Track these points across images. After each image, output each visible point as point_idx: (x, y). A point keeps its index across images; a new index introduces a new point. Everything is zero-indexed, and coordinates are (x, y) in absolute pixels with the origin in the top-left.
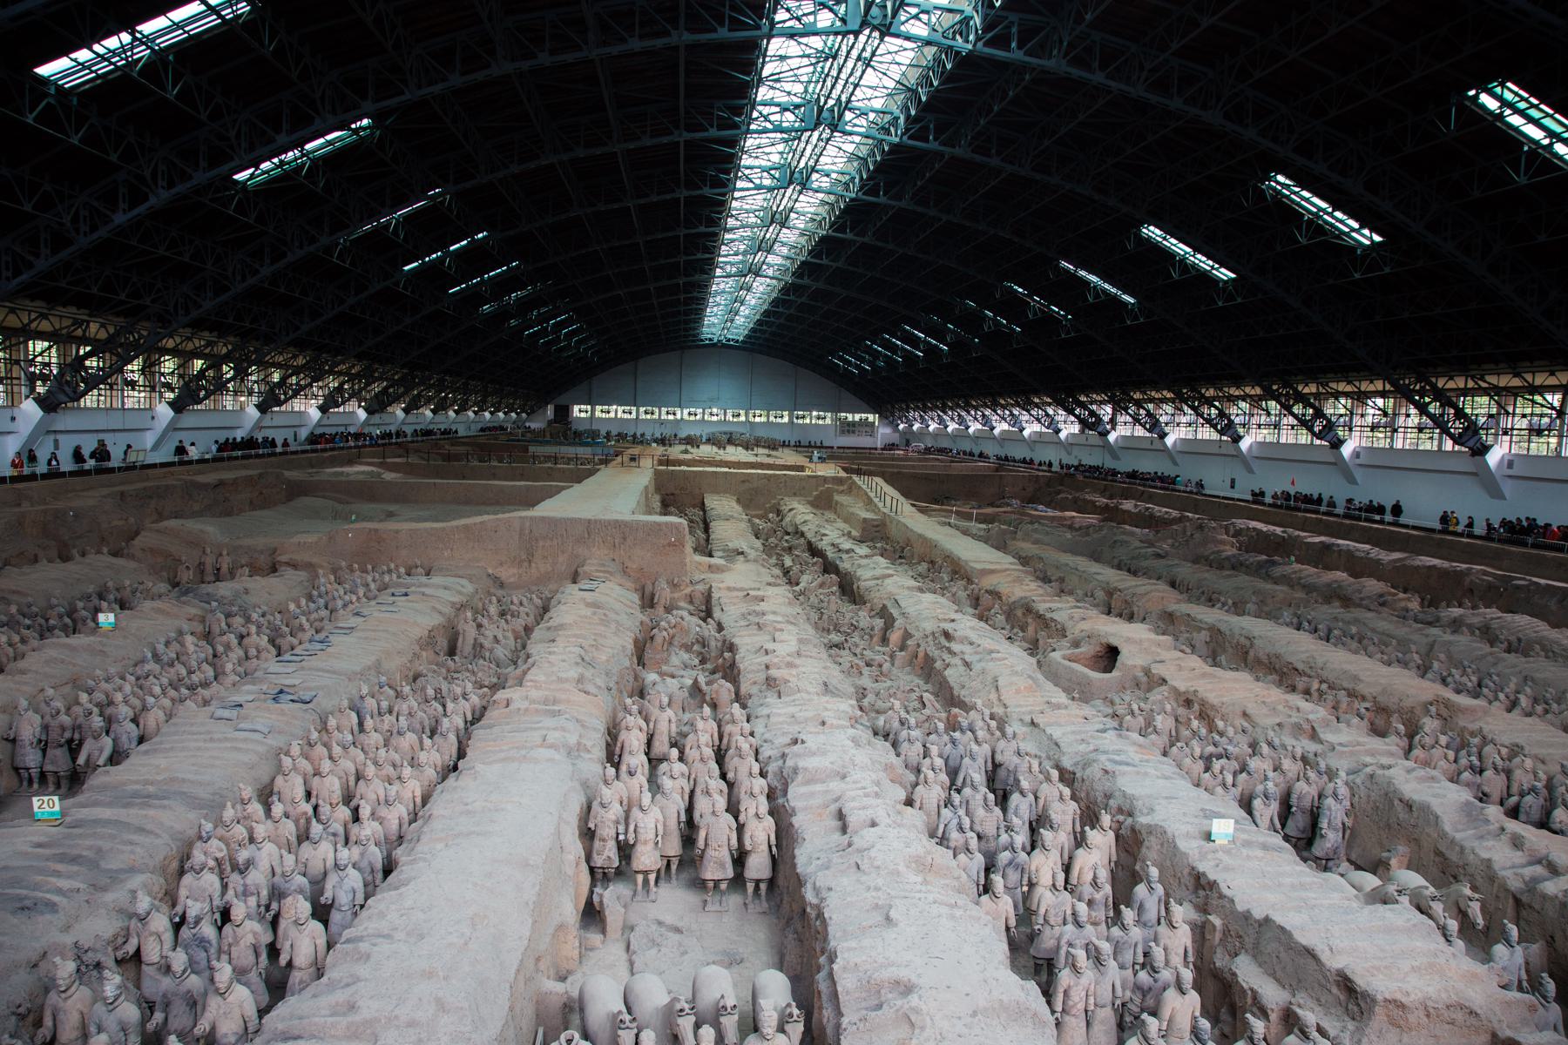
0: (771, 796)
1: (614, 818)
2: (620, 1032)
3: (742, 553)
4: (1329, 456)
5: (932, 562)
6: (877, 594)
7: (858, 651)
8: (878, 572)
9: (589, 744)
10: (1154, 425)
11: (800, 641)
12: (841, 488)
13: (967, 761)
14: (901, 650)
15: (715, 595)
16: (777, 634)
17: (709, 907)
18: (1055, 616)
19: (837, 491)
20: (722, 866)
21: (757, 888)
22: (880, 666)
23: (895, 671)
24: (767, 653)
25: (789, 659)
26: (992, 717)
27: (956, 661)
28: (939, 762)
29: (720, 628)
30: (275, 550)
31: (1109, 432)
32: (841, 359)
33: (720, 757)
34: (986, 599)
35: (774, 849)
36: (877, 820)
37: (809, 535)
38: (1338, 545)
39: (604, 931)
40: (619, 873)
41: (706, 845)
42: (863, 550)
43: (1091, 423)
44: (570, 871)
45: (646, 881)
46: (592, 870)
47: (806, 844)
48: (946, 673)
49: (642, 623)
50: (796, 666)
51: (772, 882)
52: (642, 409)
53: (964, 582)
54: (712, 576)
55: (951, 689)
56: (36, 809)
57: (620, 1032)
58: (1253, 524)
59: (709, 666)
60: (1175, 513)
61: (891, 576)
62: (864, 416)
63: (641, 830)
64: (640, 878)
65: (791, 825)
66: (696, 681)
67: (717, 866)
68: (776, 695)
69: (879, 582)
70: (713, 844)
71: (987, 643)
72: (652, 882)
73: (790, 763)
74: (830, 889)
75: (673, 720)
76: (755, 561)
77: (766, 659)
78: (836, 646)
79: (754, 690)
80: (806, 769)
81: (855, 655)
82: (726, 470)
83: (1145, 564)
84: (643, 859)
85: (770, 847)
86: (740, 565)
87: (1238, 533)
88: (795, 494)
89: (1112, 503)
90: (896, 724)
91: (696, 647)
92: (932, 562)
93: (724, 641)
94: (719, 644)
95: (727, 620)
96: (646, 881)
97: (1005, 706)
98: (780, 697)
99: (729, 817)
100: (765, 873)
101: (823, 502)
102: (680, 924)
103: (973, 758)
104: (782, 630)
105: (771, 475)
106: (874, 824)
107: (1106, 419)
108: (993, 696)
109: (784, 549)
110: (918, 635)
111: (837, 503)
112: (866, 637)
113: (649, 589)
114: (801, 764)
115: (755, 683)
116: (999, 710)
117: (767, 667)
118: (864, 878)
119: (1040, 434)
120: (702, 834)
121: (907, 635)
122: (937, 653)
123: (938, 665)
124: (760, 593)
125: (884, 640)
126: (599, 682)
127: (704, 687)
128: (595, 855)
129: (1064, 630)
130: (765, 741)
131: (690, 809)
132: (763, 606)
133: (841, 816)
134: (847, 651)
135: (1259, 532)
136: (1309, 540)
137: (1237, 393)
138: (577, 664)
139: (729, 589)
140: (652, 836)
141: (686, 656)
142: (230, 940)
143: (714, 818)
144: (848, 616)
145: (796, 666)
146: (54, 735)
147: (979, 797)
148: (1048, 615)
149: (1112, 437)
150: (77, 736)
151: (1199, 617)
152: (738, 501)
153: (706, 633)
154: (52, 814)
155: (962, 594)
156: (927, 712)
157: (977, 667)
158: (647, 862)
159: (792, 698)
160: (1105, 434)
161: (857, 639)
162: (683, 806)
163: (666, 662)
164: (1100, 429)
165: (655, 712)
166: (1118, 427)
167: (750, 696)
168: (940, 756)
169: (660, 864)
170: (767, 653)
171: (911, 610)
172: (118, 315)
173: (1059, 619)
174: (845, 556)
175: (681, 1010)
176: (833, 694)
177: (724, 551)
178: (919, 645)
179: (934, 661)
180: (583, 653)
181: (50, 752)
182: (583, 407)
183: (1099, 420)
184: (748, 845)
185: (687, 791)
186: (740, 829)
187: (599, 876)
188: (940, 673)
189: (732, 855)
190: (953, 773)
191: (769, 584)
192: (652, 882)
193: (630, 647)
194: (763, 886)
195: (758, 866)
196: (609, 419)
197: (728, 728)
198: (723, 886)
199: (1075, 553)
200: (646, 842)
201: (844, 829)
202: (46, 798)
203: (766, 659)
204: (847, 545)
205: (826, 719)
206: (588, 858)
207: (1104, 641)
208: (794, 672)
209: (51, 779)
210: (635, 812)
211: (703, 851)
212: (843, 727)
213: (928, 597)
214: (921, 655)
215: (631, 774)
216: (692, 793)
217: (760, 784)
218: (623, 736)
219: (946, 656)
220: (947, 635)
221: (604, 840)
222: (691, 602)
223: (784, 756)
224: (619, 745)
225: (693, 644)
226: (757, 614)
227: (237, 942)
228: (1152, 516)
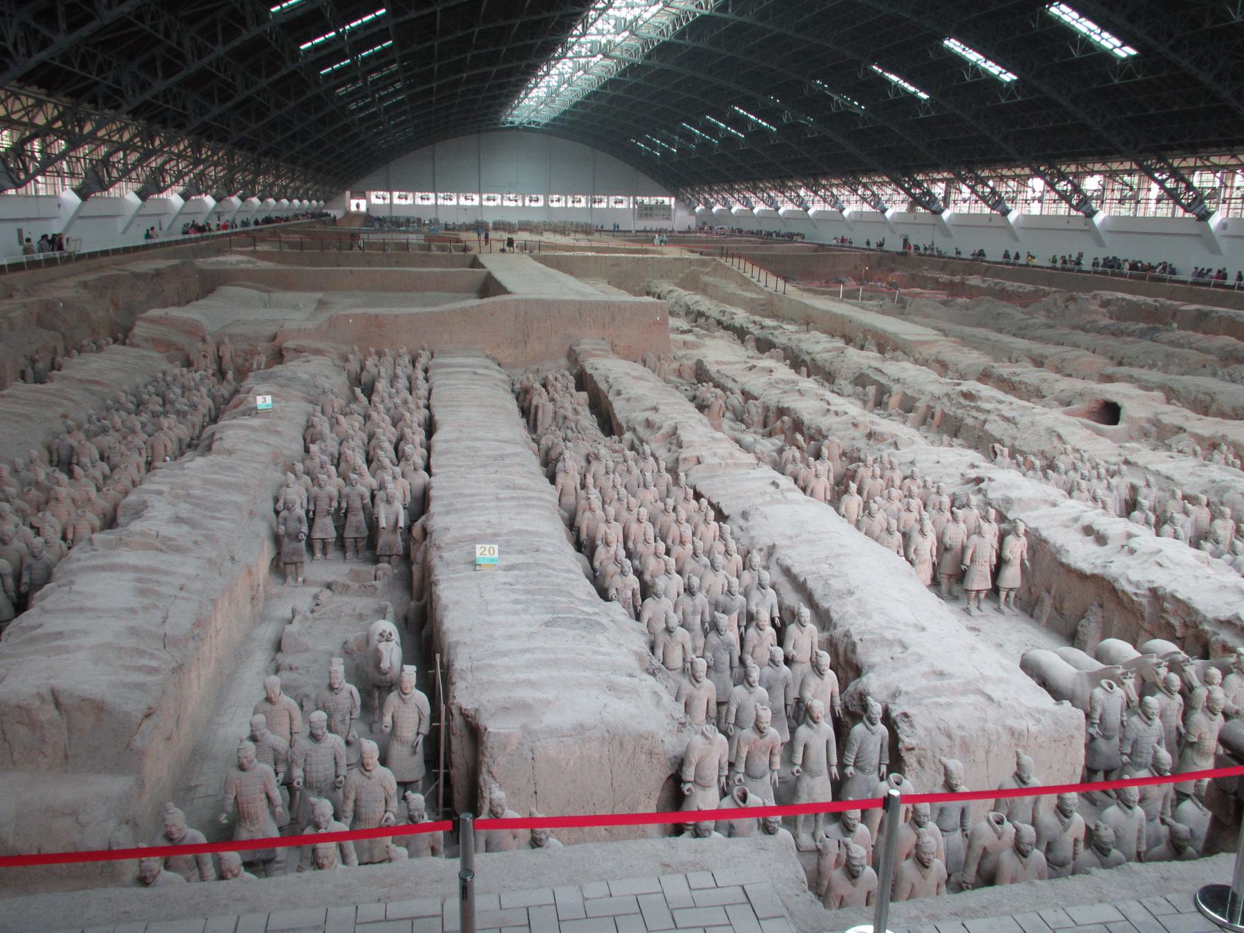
1: (897, 543)
4: (1196, 228)
10: (996, 201)
12: (709, 269)
15: (712, 369)
18: (1025, 380)
19: (702, 272)
20: (987, 580)
21: (1007, 596)
24: (837, 413)
27: (992, 417)
29: (747, 395)
30: (274, 338)
31: (942, 211)
32: (649, 143)
35: (1027, 562)
38: (1217, 312)
41: (972, 560)
43: (923, 200)
52: (485, 196)
53: (899, 353)
56: (478, 555)
57: (1125, 681)
58: (1120, 295)
60: (1029, 288)
62: (660, 199)
65: (1045, 541)
67: (980, 580)
70: (979, 560)
80: (1020, 499)
82: (594, 254)
83: (1038, 333)
85: (1022, 560)
87: (1106, 304)
88: (662, 277)
89: (957, 279)
93: (767, 409)
94: (760, 410)
98: (897, 449)
101: (691, 283)
105: (639, 259)
107: (940, 197)
111: (706, 285)
117: (855, 425)
119: (861, 214)
133: (1088, 530)
135: (1129, 302)
136: (1184, 308)
137: (1121, 167)
142: (755, 642)
146: (323, 505)
148: (1014, 379)
149: (946, 215)
150: (344, 505)
151: (1144, 377)
152: (609, 283)
154: (492, 560)
157: (1024, 420)
160: (938, 212)
164: (934, 208)
166: (952, 205)
172: (66, 96)
173: (1029, 382)
174: (775, 332)
181: (319, 522)
182: (381, 193)
183: (933, 199)
189: (991, 571)
194: (1012, 594)
195: (1012, 577)
196: (473, 207)
198: (982, 595)
199: (979, 325)
200: (924, 562)
202: (488, 546)
204: (768, 322)
205: (976, 463)
207: (1100, 398)
209: (318, 546)
214: (938, 415)
219: (975, 414)
220: (967, 396)
222: (680, 375)
227: (760, 644)
228: (1003, 290)
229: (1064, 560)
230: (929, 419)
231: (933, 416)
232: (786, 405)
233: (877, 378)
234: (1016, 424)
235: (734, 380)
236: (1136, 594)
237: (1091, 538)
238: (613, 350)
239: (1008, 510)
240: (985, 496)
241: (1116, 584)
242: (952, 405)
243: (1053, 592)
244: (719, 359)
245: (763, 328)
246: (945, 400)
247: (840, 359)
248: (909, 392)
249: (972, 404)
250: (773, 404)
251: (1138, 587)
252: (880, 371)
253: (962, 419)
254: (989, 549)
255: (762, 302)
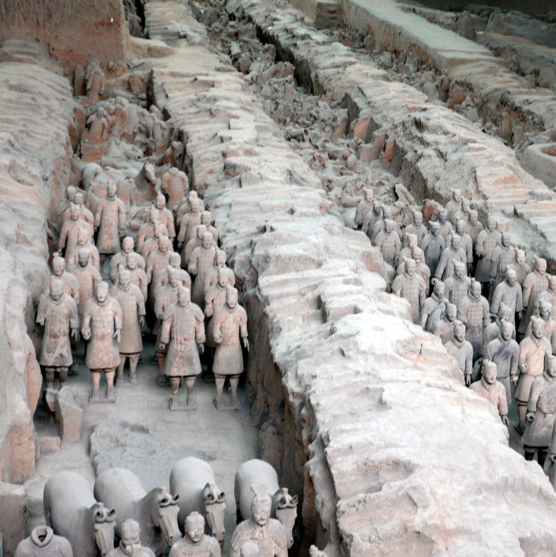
0: (239, 284)
1: (66, 311)
2: (97, 526)
3: (185, 37)
5: (396, 52)
6: (339, 83)
7: (319, 143)
8: (338, 60)
9: (29, 235)
11: (259, 129)
13: (447, 250)
14: (367, 142)
15: (158, 81)
16: (232, 121)
17: (175, 406)
20: (189, 360)
21: (227, 384)
22: (345, 158)
23: (361, 164)
24: (222, 140)
25: (249, 147)
26: (472, 207)
27: (429, 151)
28: (419, 251)
29: (166, 115)
33: (178, 247)
34: (456, 91)
35: (246, 342)
36: (360, 307)
37: (259, 20)
39: (60, 434)
40: (72, 374)
41: (171, 338)
42: (319, 37)
44: (21, 368)
45: (104, 381)
46: (43, 369)
47: (285, 334)
48: (419, 164)
49: (75, 110)
50: (255, 154)
51: (243, 378)
54: (154, 61)
55: (425, 181)
57: (97, 526)
59: (155, 157)
61: (354, 63)
63: (97, 324)
64: (97, 377)
65: (265, 315)
66: (144, 172)
68: (236, 184)
69: (340, 70)
70: (178, 337)
71: (462, 133)
72: (111, 382)
73: (259, 251)
74: (314, 377)
75: (123, 210)
76: (200, 44)
77: (222, 147)
78: (295, 138)
79: (211, 179)
80: (278, 257)
81: (316, 147)
84: (100, 355)
85: (241, 339)
86: (183, 48)
90: (370, 214)
91: (140, 138)
92: (396, 52)
94: (166, 133)
95: (171, 107)
96: (104, 381)
97: (485, 197)
98: (241, 186)
99: (196, 308)
100: (236, 368)
102: (144, 424)
103: (454, 248)
104: (237, 117)
106: (356, 311)
108: (471, 187)
109: (230, 35)
110: (386, 126)
112: (328, 129)
113: (80, 74)
114: (272, 251)
115: (211, 172)
116: (479, 202)
117: (224, 155)
118: (350, 364)
120: (166, 327)
121: (373, 126)
122: (409, 143)
123: (410, 156)
124: (209, 78)
125: (348, 132)
126: (36, 170)
127: (153, 177)
128: (45, 354)
129: (542, 123)
130: (229, 231)
131: (150, 303)
132: (213, 92)
133: (320, 303)
134: (307, 144)
138: (7, 151)
139: (173, 74)
140: (110, 330)
141: (128, 147)
143: (180, 309)
144: (307, 106)
145: (255, 154)
147: (463, 287)
153: (150, 122)
155: (430, 86)
156: (401, 203)
158: (106, 359)
159: (254, 187)
161: (316, 131)
162: (142, 297)
163: (105, 152)
165: (100, 200)
167: (206, 186)
168: (419, 245)
169: (120, 362)
170: (222, 140)
171: (377, 99)
174: (299, 42)
175: (164, 501)
176: (297, 182)
177: (163, 34)
178: (387, 137)
179: (404, 152)
180: (12, 139)
184: (217, 334)
185: (146, 282)
186: (208, 321)
187: (51, 376)
188: (411, 165)
190: (434, 265)
191: (219, 70)
192: (111, 382)
193: (65, 136)
194: (234, 382)
197: (185, 218)
198: (191, 383)
200: (103, 337)
201: (324, 317)
203: (222, 147)
206: (39, 356)
208: (255, 159)
210: (92, 306)
211: (167, 346)
212: (314, 215)
213: (395, 87)
214: (389, 146)
215: (82, 265)
216: (150, 286)
217: (227, 274)
218: (67, 227)
221: (55, 336)
223: (252, 244)
224: (63, 237)
225: (135, 134)
226: (208, 100)
229: (271, 342)
230: (382, 152)
231: (385, 149)
232: (181, 129)
233: (356, 100)
234: (446, 161)
235: (167, 97)
236: (293, 393)
237: (319, 311)
238: (51, 55)
239: (263, 270)
240: (253, 251)
241: (284, 379)
242: (405, 135)
243: (265, 382)
244: (177, 70)
245: (294, 36)
246: (399, 129)
247: (337, 76)
248: (377, 119)
249: (419, 135)
250: (176, 126)
251: (300, 383)
252: (362, 92)
253: (406, 153)
254: (194, 322)
255: (332, 9)
